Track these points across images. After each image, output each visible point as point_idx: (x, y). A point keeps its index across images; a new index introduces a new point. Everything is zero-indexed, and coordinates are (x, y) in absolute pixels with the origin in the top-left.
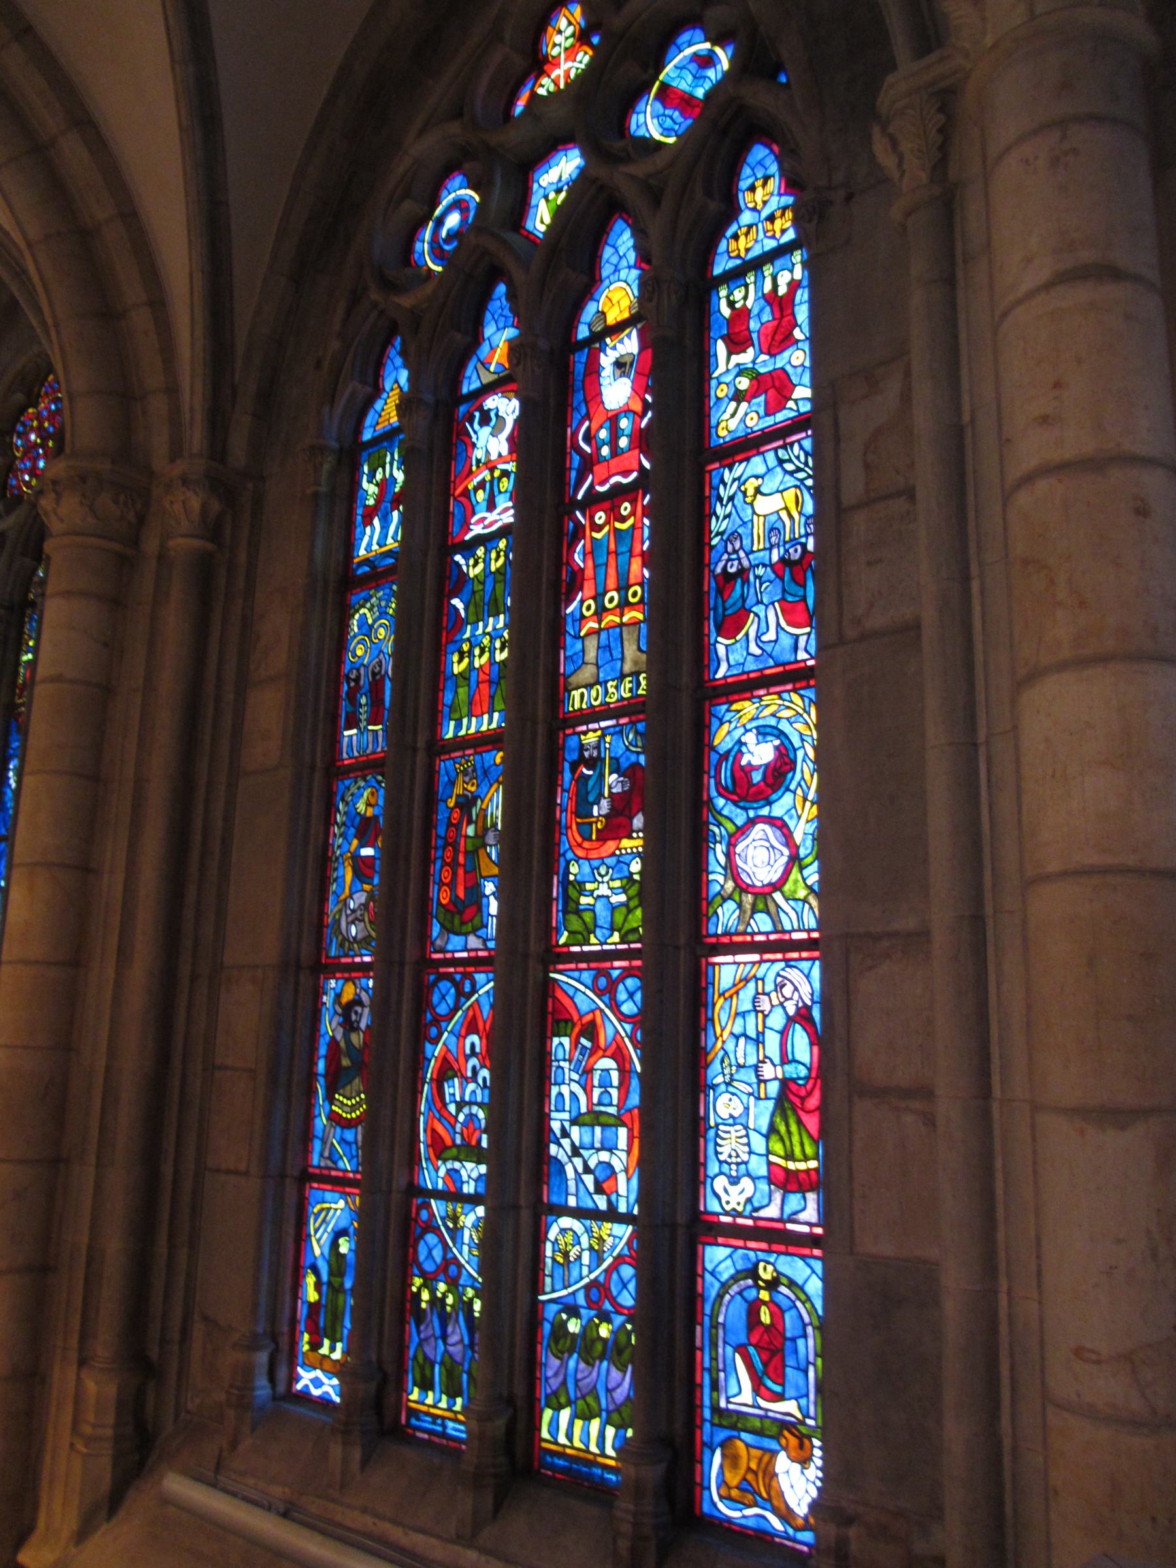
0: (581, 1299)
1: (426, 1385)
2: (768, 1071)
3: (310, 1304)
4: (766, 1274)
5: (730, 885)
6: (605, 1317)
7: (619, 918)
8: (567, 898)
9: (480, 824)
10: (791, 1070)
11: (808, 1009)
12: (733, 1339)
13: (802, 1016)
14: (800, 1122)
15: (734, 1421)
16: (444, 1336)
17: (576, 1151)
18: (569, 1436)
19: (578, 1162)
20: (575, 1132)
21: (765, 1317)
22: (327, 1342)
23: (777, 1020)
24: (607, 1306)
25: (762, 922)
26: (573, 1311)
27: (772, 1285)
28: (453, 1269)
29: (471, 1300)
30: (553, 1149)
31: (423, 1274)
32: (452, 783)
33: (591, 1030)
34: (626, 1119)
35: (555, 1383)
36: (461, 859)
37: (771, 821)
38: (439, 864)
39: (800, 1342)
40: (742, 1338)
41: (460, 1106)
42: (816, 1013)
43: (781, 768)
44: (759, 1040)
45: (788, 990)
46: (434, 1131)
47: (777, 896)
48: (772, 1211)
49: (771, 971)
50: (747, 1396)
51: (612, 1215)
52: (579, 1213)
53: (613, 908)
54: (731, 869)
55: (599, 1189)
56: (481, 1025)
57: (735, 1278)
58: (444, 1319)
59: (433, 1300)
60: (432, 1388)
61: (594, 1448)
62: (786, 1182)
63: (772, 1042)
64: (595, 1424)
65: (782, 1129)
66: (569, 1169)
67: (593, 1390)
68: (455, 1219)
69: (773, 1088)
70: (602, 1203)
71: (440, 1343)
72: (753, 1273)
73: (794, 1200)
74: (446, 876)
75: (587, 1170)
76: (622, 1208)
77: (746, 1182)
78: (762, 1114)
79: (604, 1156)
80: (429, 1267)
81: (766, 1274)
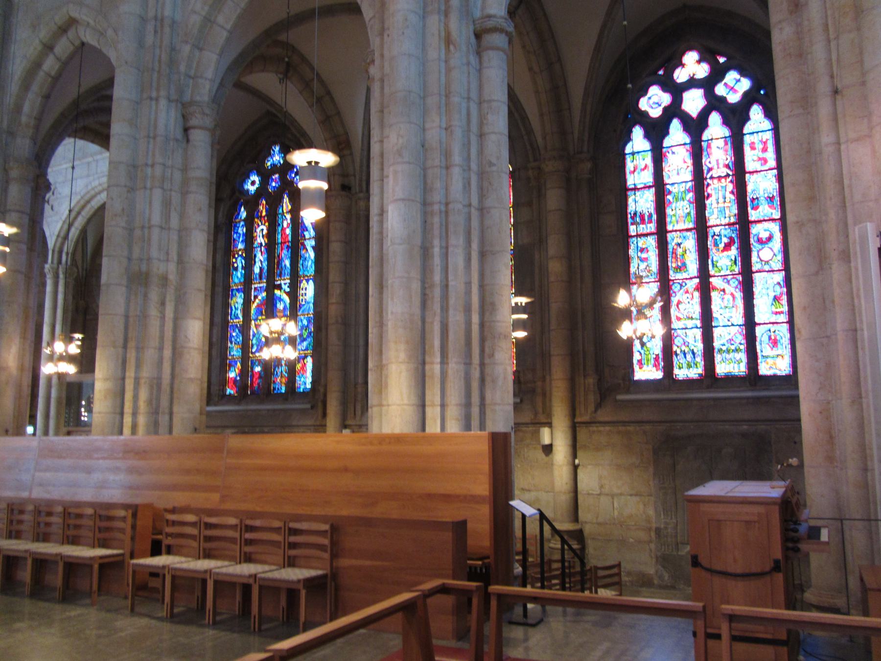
4: (772, 330)
5: (759, 260)
7: (729, 267)
9: (684, 249)
12: (765, 343)
14: (778, 302)
15: (767, 357)
16: (685, 357)
21: (773, 338)
24: (732, 342)
26: (724, 345)
27: (774, 332)
28: (687, 344)
32: (673, 240)
33: (724, 290)
36: (679, 256)
38: (671, 258)
39: (781, 340)
40: (768, 342)
46: (677, 316)
47: (770, 262)
58: (685, 354)
59: (681, 351)
65: (774, 303)
67: (731, 359)
68: (686, 333)
71: (684, 359)
74: (674, 260)
81: (772, 330)
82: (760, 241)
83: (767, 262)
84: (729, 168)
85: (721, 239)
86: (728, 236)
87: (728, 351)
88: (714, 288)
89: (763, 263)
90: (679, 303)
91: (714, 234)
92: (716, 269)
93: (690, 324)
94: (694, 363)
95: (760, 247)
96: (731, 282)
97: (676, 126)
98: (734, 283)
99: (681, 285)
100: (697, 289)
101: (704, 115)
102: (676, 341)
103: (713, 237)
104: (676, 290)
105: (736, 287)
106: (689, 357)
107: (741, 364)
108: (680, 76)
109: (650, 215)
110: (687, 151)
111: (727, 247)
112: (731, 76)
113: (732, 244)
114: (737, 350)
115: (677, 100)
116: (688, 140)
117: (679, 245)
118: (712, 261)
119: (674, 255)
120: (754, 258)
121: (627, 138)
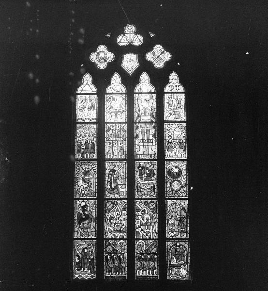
0: (144, 252)
1: (109, 272)
2: (178, 217)
3: (77, 263)
6: (149, 254)
8: (138, 189)
10: (182, 216)
11: (184, 208)
13: (184, 209)
16: (114, 263)
17: (142, 230)
18: (143, 273)
19: (143, 232)
20: (142, 227)
22: (82, 269)
23: (179, 209)
25: (176, 195)
27: (179, 246)
29: (120, 256)
30: (137, 230)
31: (108, 253)
33: (144, 211)
34: (152, 224)
35: (139, 266)
37: (178, 181)
41: (115, 224)
42: (186, 209)
43: (179, 174)
44: (176, 212)
45: (181, 205)
48: (179, 236)
49: (178, 203)
50: (175, 261)
51: (150, 239)
52: (143, 239)
53: (148, 191)
54: (171, 187)
55: (147, 235)
56: (119, 210)
57: (173, 246)
59: (111, 257)
60: (111, 272)
61: (147, 274)
62: (182, 232)
63: (179, 212)
64: (148, 271)
66: (141, 233)
69: (179, 219)
70: (148, 237)
72: (176, 245)
73: (182, 234)
75: (144, 232)
76: (152, 238)
77: (175, 232)
78: (177, 223)
79: (148, 230)
80: (109, 251)
82: (172, 175)
83: (176, 192)
84: (153, 117)
85: (145, 170)
86: (149, 169)
87: (145, 260)
88: (138, 210)
89: (174, 192)
90: (111, 218)
91: (140, 166)
92: (140, 193)
93: (118, 235)
94: (120, 268)
95: (172, 180)
96: (150, 205)
97: (116, 78)
98: (152, 206)
99: (114, 204)
100: (124, 209)
101: (138, 73)
102: (107, 249)
103: (138, 168)
104: (110, 207)
105: (154, 209)
106: (116, 262)
107: (155, 271)
108: (122, 41)
109: (93, 148)
110: (124, 99)
111: (149, 176)
112: (158, 48)
113: (152, 175)
114: (152, 259)
115: (118, 60)
116: (124, 91)
117: (114, 171)
118: (137, 187)
119: (109, 179)
120: (168, 188)
121: (78, 81)
